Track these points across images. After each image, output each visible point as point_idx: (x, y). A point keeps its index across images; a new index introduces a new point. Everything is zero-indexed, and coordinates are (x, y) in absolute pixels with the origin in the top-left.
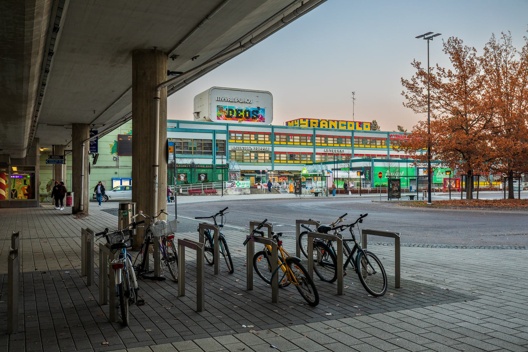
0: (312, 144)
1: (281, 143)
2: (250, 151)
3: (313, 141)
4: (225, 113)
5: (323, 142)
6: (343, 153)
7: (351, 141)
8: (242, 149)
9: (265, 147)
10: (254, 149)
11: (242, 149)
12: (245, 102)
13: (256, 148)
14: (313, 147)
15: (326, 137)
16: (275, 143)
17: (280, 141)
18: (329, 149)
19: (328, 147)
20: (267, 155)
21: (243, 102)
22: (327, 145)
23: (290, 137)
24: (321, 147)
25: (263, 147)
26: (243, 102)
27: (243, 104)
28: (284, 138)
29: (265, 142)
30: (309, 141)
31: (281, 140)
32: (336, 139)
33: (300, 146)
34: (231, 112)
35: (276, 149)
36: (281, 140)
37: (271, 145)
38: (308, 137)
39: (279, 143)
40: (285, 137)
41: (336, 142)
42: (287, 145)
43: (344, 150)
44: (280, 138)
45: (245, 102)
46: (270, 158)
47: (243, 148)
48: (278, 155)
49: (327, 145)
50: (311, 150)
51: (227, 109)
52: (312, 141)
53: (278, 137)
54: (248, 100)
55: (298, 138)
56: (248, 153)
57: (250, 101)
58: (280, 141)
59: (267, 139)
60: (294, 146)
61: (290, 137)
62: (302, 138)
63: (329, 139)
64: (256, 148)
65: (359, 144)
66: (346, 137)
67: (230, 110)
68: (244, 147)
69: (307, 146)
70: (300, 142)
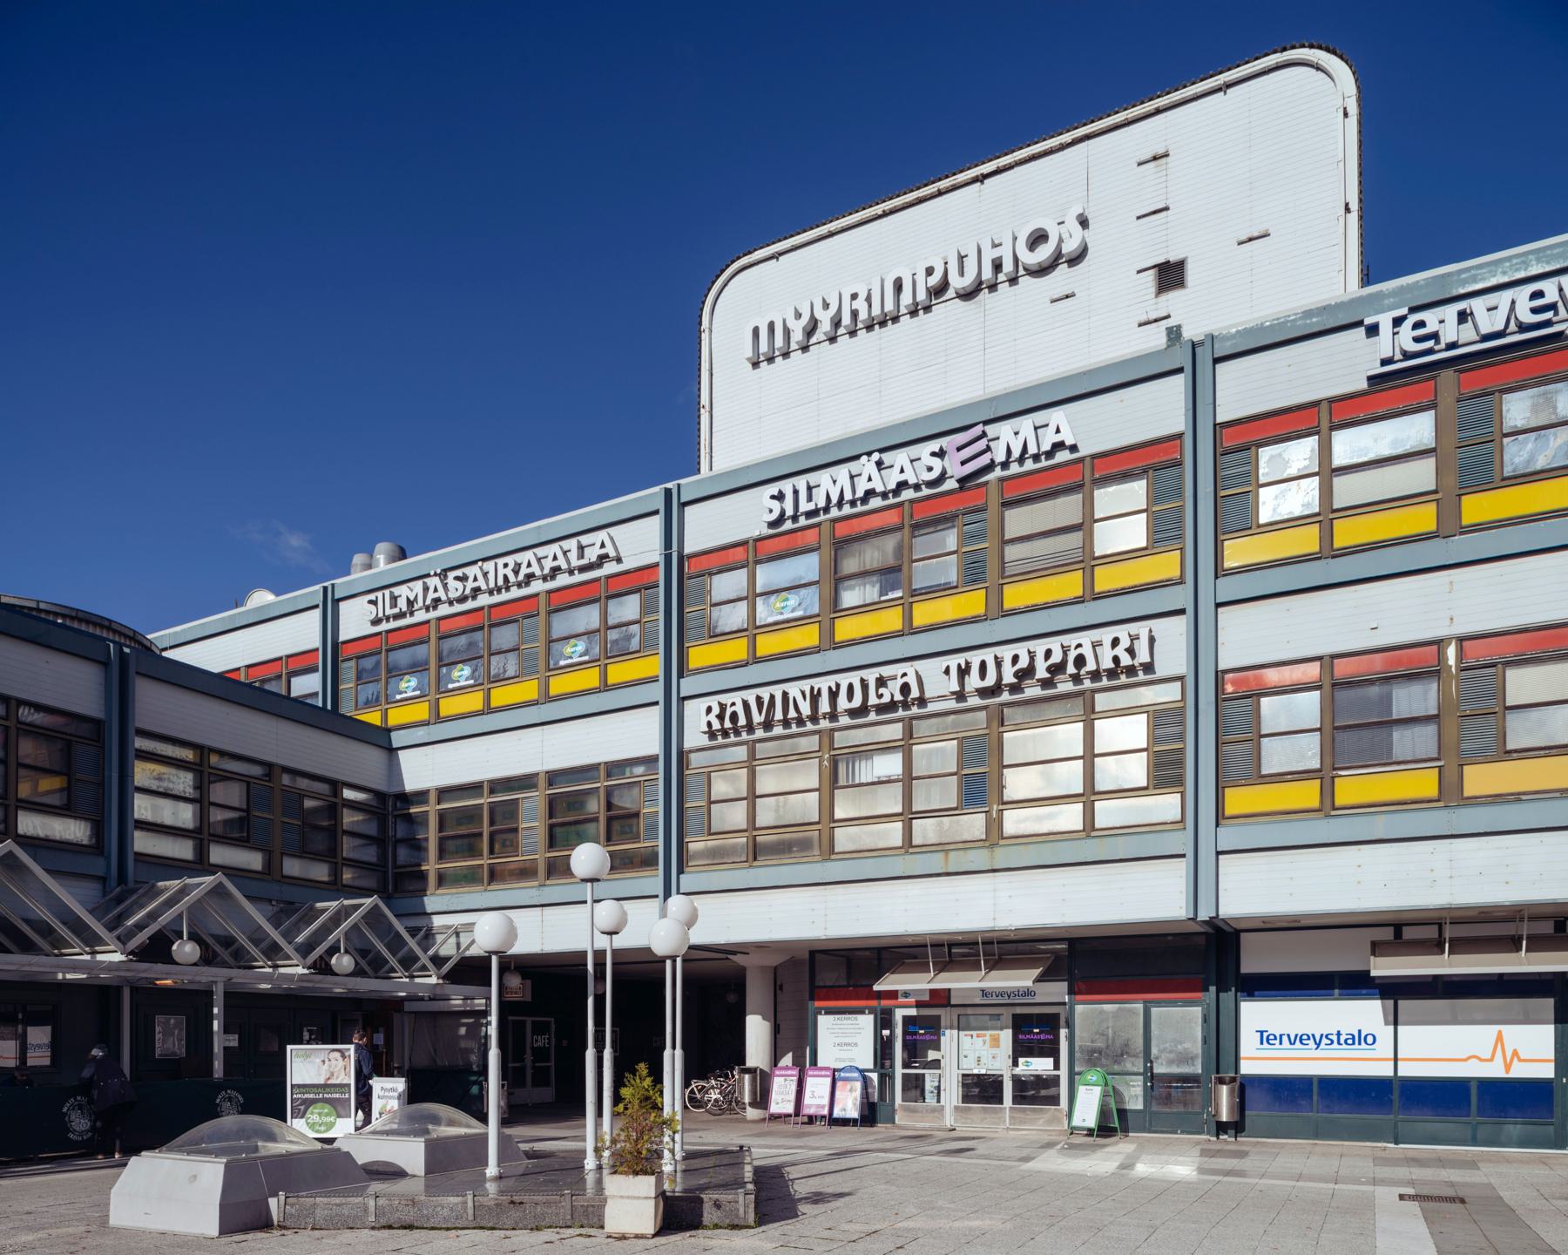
8: (806, 709)
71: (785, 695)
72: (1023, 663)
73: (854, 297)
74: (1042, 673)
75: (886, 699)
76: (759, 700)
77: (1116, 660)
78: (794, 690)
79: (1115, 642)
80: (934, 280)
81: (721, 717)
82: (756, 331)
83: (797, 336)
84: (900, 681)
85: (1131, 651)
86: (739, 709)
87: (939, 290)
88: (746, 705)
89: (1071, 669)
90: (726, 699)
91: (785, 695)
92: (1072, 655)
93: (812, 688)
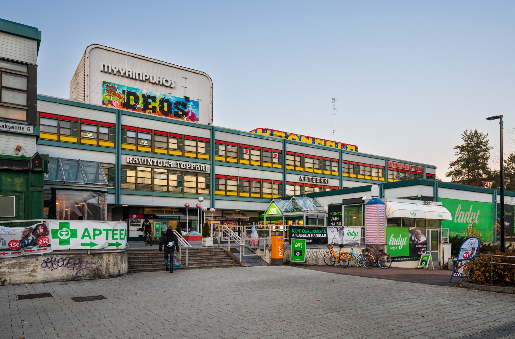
0: (280, 166)
1: (229, 160)
2: (168, 170)
3: (282, 161)
4: (120, 98)
5: (298, 164)
6: (328, 185)
7: (338, 167)
8: (151, 164)
9: (198, 165)
10: (175, 166)
11: (151, 164)
12: (161, 83)
13: (180, 165)
14: (282, 171)
15: (303, 156)
16: (217, 158)
17: (226, 156)
18: (307, 177)
19: (306, 174)
20: (202, 179)
21: (157, 82)
22: (304, 169)
23: (244, 150)
24: (294, 172)
25: (194, 164)
26: (157, 82)
27: (158, 88)
28: (234, 150)
29: (197, 156)
30: (275, 160)
31: (229, 154)
32: (317, 162)
33: (262, 168)
34: (132, 98)
35: (219, 170)
36: (229, 154)
37: (209, 162)
38: (274, 154)
39: (224, 159)
40: (234, 149)
41: (317, 166)
42: (238, 165)
43: (329, 179)
44: (226, 151)
45: (161, 83)
46: (207, 187)
47: (153, 162)
48: (222, 182)
49: (304, 169)
50: (279, 177)
51: (124, 92)
52: (281, 161)
53: (222, 147)
54: (166, 81)
55: (258, 153)
56: (164, 173)
57: (172, 84)
58: (226, 156)
59: (202, 150)
60: (250, 166)
61: (244, 150)
62: (265, 154)
63: (307, 160)
64: (180, 165)
65: (349, 173)
66: (331, 160)
67: (130, 94)
68: (155, 160)
69: (272, 169)
70: (261, 161)
71: (147, 160)
73: (129, 72)
74: (192, 168)
75: (167, 166)
76: (141, 159)
77: (203, 169)
78: (149, 160)
79: (203, 167)
80: (147, 78)
81: (132, 161)
82: (104, 66)
83: (115, 72)
84: (169, 164)
85: (205, 168)
86: (137, 160)
89: (196, 169)
90: (135, 157)
91: (147, 160)
92: (197, 167)
93: (153, 160)
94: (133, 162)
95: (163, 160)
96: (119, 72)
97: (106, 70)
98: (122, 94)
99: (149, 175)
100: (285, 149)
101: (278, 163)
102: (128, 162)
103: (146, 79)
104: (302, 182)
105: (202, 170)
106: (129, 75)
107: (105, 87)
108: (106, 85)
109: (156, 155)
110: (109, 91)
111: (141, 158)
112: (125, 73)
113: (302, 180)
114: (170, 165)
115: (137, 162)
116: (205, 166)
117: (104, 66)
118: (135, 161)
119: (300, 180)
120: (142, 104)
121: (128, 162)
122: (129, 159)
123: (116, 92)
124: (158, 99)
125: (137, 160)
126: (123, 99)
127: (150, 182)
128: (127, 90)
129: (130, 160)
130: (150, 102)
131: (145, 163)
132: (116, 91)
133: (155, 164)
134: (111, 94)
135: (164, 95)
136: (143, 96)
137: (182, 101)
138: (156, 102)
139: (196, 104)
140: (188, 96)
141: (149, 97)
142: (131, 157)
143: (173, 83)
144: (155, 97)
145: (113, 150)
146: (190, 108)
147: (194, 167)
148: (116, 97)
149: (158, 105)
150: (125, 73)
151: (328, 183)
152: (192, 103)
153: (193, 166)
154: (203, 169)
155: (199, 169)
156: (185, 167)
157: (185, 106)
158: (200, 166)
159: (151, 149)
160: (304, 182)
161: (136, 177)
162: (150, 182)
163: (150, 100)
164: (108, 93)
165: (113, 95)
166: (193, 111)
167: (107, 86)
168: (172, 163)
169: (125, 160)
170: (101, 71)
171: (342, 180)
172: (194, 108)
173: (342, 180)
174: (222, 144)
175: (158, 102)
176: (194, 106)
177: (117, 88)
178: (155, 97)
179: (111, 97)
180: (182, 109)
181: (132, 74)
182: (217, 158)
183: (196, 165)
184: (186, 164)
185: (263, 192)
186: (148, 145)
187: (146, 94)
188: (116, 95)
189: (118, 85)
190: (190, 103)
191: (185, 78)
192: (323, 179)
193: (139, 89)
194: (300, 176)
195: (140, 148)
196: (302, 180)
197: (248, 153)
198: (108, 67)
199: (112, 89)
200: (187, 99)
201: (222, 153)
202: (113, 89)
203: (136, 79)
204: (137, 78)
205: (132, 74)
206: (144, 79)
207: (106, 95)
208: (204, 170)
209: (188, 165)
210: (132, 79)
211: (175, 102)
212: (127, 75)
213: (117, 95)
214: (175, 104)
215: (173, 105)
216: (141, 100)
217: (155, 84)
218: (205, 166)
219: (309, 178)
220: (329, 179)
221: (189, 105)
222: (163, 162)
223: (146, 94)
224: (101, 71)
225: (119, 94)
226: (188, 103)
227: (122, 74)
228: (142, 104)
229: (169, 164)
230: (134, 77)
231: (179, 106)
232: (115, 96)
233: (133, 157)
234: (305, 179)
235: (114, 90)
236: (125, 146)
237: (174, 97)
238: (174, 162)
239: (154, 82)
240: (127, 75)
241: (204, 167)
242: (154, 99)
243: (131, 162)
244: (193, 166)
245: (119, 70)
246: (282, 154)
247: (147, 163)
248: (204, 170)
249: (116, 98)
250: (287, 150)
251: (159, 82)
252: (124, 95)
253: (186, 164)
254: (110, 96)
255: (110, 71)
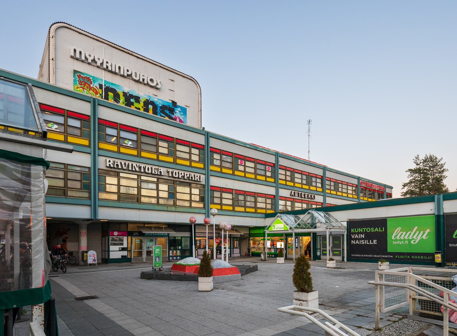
0: (272, 180)
1: (224, 170)
2: (158, 179)
3: (275, 175)
4: (97, 93)
5: (289, 178)
7: (322, 184)
8: (137, 169)
9: (193, 174)
10: (167, 174)
11: (137, 169)
12: (146, 82)
13: (172, 173)
15: (293, 171)
16: (212, 168)
17: (221, 167)
21: (141, 80)
22: (294, 184)
23: (239, 161)
24: (286, 187)
26: (141, 80)
27: (142, 87)
28: (229, 160)
29: (190, 164)
30: (269, 174)
31: (224, 164)
32: (304, 177)
33: (256, 181)
34: (111, 94)
35: (215, 182)
36: (224, 164)
37: (204, 172)
38: (267, 167)
39: (219, 169)
40: (229, 159)
41: (304, 182)
42: (233, 177)
43: (316, 196)
44: (221, 160)
46: (202, 199)
49: (294, 184)
50: (271, 191)
51: (101, 86)
52: (273, 175)
53: (216, 156)
54: (152, 80)
55: (252, 165)
56: (153, 182)
57: (157, 84)
58: (221, 167)
59: (195, 158)
60: (245, 179)
61: (239, 161)
62: (259, 166)
63: (297, 175)
64: (172, 173)
65: (330, 190)
66: (316, 176)
67: (108, 90)
68: (142, 165)
69: (265, 183)
70: (256, 174)
71: (132, 165)
72: (183, 175)
74: (186, 178)
75: (156, 173)
76: (125, 164)
77: (197, 179)
78: (134, 164)
79: (197, 176)
80: (129, 73)
82: (75, 51)
83: (90, 61)
85: (200, 178)
86: (119, 164)
87: (130, 76)
88: (121, 163)
89: (190, 179)
90: (116, 160)
91: (132, 165)
92: (191, 176)
93: (139, 166)
94: (114, 166)
95: (152, 166)
96: (94, 60)
97: (78, 56)
98: (99, 88)
99: (135, 184)
100: (278, 163)
101: (271, 177)
102: (108, 165)
103: (128, 75)
104: (292, 197)
105: (196, 180)
106: (107, 67)
107: (77, 77)
108: (77, 75)
109: (143, 159)
110: (82, 83)
111: (125, 161)
112: (102, 64)
113: (293, 195)
114: (160, 172)
115: (120, 167)
116: (200, 176)
117: (75, 51)
118: (117, 165)
119: (291, 195)
120: (123, 103)
121: (108, 165)
122: (110, 161)
123: (92, 86)
124: (142, 100)
125: (119, 164)
126: (100, 94)
127: (136, 192)
128: (105, 85)
129: (110, 163)
130: (133, 103)
131: (130, 169)
132: (91, 84)
133: (142, 170)
134: (84, 86)
135: (149, 96)
136: (125, 94)
137: (169, 106)
138: (140, 103)
139: (184, 111)
140: (176, 101)
141: (131, 96)
142: (112, 160)
143: (159, 83)
144: (139, 98)
145: (88, 150)
146: (178, 113)
147: (188, 176)
148: (91, 91)
149: (142, 107)
150: (102, 64)
151: (314, 199)
152: (179, 109)
153: (187, 175)
154: (197, 179)
155: (193, 179)
156: (177, 176)
157: (172, 111)
158: (194, 175)
159: (136, 151)
160: (294, 197)
161: (119, 185)
162: (136, 192)
163: (132, 100)
164: (81, 85)
165: (88, 88)
166: (180, 118)
167: (79, 76)
168: (163, 170)
169: (102, 163)
170: (72, 57)
171: (325, 196)
172: (182, 115)
173: (325, 196)
174: (217, 153)
175: (142, 104)
176: (182, 112)
177: (92, 81)
178: (139, 98)
179: (85, 90)
180: (169, 114)
181: (111, 66)
182: (212, 168)
183: (190, 174)
184: (179, 173)
185: (258, 207)
186: (132, 146)
187: (128, 92)
188: (90, 89)
189: (93, 77)
190: (177, 109)
191: (172, 80)
192: (311, 194)
193: (119, 86)
194: (292, 191)
195: (122, 150)
196: (293, 195)
197: (243, 164)
198: (80, 53)
199: (86, 81)
200: (174, 103)
201: (217, 163)
202: (88, 81)
203: (115, 73)
204: (117, 71)
205: (111, 66)
206: (126, 75)
207: (79, 88)
208: (199, 180)
209: (181, 174)
210: (111, 72)
211: (161, 105)
212: (105, 66)
213: (92, 89)
214: (161, 107)
215: (159, 109)
216: (122, 99)
217: (138, 81)
218: (200, 176)
219: (298, 193)
220: (316, 196)
221: (176, 111)
222: (152, 168)
223: (128, 92)
224: (72, 57)
225: (95, 87)
226: (175, 109)
227: (99, 64)
228: (123, 103)
229: (159, 171)
230: (113, 70)
231: (166, 111)
232: (90, 90)
233: (114, 160)
234: (296, 194)
235: (89, 83)
236: (103, 146)
237: (160, 100)
238: (166, 169)
239: (137, 79)
240: (105, 66)
241: (199, 177)
242: (137, 99)
243: (112, 166)
244: (187, 175)
245: (94, 59)
246: (275, 167)
247: (132, 168)
248: (199, 180)
249: (91, 92)
250: (280, 163)
251: (143, 80)
252: (101, 90)
253: (179, 173)
254: (83, 89)
255: (83, 58)
